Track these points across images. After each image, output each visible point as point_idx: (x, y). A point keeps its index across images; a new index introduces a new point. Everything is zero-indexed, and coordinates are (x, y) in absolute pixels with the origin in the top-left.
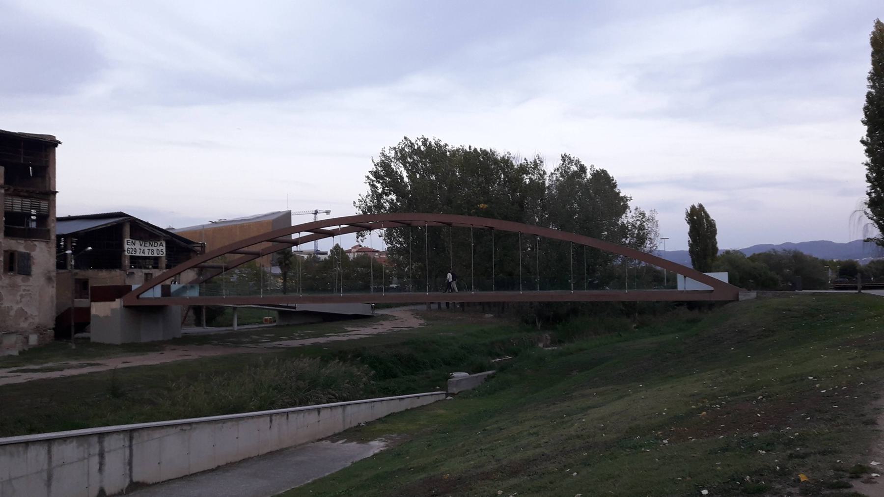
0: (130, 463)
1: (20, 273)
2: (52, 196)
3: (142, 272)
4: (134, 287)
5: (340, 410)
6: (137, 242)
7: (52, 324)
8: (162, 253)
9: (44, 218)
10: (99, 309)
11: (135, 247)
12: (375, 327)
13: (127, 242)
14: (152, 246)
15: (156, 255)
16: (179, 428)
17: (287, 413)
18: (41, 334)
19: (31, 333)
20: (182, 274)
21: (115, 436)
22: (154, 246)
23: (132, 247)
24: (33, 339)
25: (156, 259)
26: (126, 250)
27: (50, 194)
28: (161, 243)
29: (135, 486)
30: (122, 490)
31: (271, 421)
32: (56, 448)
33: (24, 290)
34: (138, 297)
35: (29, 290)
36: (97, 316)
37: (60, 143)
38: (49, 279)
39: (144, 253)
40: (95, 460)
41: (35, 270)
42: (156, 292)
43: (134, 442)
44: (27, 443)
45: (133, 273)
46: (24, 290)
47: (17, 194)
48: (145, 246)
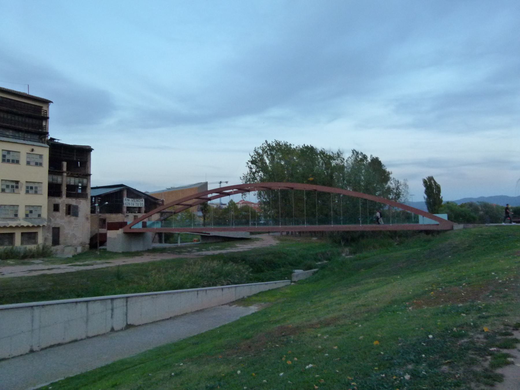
0: (126, 315)
1: (73, 216)
2: (89, 177)
4: (128, 223)
5: (233, 289)
6: (131, 199)
7: (88, 241)
9: (84, 188)
10: (111, 234)
11: (130, 202)
12: (251, 244)
14: (138, 201)
15: (139, 206)
16: (151, 296)
17: (206, 290)
18: (83, 247)
19: (78, 246)
20: (152, 216)
21: (119, 300)
23: (128, 202)
24: (79, 250)
25: (140, 208)
26: (125, 203)
27: (88, 175)
29: (129, 326)
30: (123, 328)
31: (198, 294)
32: (91, 305)
33: (75, 224)
34: (130, 228)
35: (77, 224)
36: (110, 238)
37: (93, 149)
38: (87, 219)
40: (110, 311)
41: (81, 214)
42: (139, 226)
43: (128, 303)
44: (76, 302)
45: (128, 216)
46: (75, 224)
47: (72, 176)
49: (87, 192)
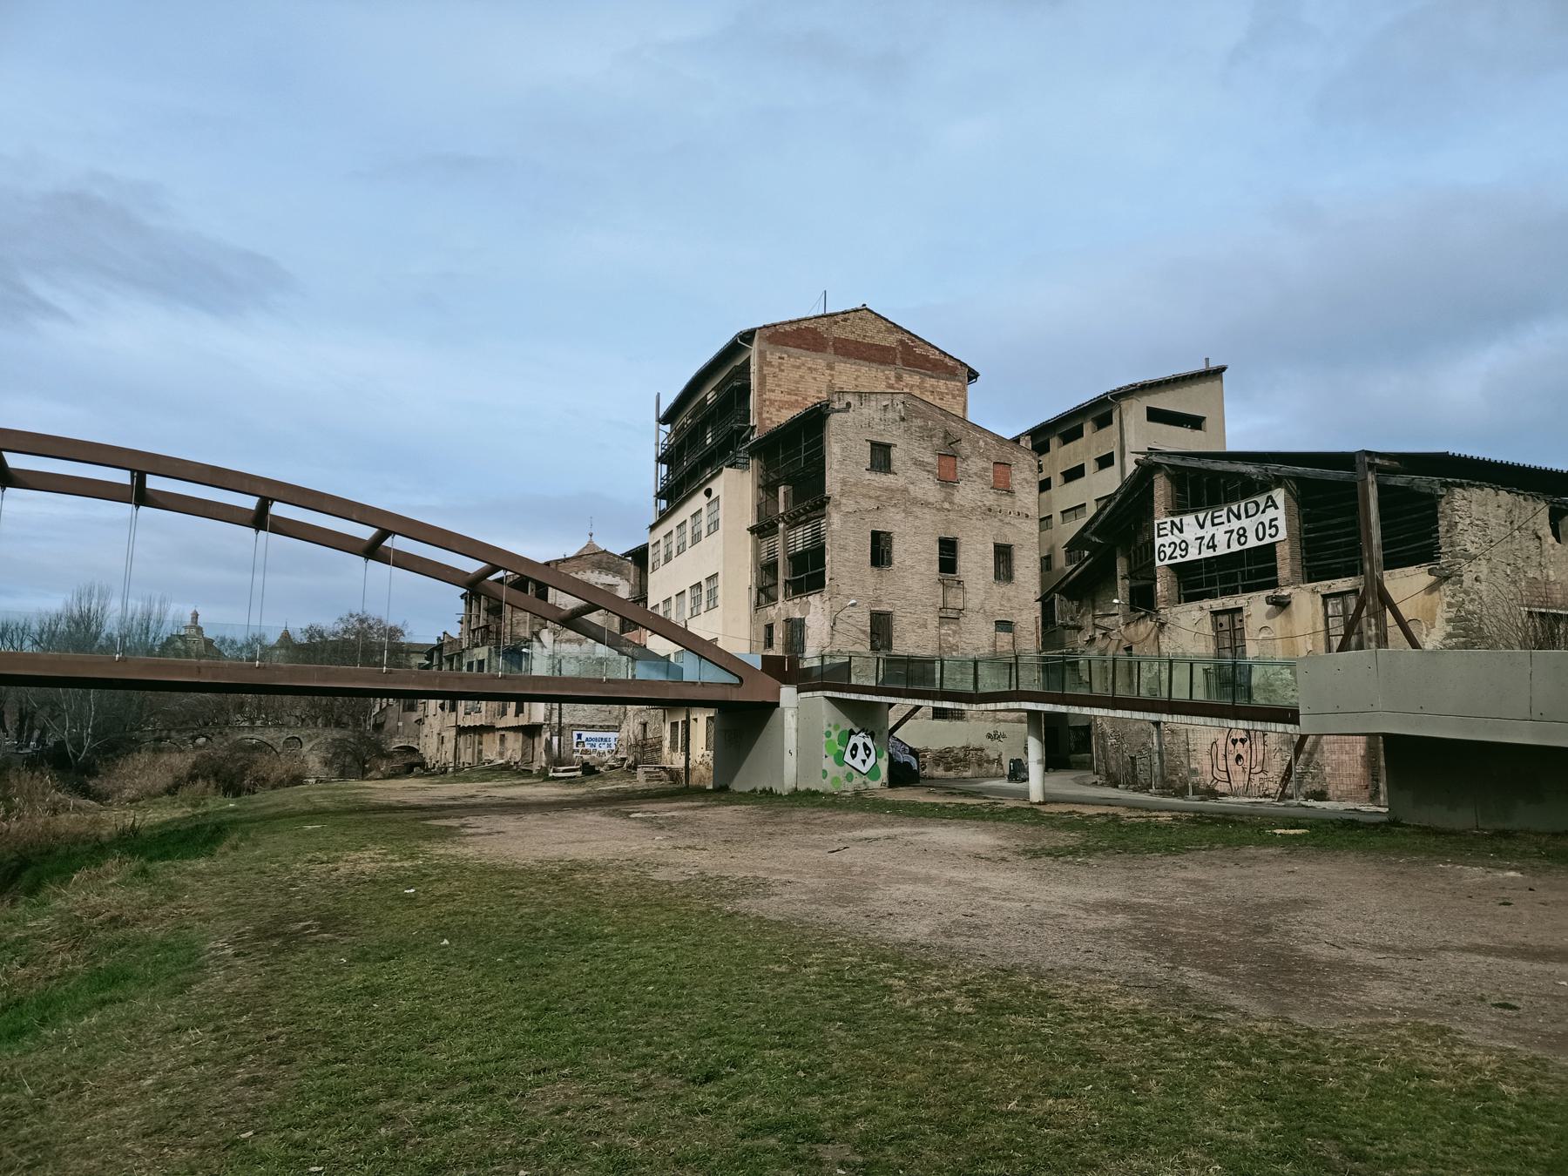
3: (1202, 609)
6: (1189, 520)
8: (1273, 531)
11: (1184, 536)
13: (1159, 530)
14: (1238, 517)
15: (1252, 542)
20: (656, 635)
22: (1247, 517)
28: (1270, 498)
39: (1214, 547)
48: (1213, 525)
49: (241, 638)
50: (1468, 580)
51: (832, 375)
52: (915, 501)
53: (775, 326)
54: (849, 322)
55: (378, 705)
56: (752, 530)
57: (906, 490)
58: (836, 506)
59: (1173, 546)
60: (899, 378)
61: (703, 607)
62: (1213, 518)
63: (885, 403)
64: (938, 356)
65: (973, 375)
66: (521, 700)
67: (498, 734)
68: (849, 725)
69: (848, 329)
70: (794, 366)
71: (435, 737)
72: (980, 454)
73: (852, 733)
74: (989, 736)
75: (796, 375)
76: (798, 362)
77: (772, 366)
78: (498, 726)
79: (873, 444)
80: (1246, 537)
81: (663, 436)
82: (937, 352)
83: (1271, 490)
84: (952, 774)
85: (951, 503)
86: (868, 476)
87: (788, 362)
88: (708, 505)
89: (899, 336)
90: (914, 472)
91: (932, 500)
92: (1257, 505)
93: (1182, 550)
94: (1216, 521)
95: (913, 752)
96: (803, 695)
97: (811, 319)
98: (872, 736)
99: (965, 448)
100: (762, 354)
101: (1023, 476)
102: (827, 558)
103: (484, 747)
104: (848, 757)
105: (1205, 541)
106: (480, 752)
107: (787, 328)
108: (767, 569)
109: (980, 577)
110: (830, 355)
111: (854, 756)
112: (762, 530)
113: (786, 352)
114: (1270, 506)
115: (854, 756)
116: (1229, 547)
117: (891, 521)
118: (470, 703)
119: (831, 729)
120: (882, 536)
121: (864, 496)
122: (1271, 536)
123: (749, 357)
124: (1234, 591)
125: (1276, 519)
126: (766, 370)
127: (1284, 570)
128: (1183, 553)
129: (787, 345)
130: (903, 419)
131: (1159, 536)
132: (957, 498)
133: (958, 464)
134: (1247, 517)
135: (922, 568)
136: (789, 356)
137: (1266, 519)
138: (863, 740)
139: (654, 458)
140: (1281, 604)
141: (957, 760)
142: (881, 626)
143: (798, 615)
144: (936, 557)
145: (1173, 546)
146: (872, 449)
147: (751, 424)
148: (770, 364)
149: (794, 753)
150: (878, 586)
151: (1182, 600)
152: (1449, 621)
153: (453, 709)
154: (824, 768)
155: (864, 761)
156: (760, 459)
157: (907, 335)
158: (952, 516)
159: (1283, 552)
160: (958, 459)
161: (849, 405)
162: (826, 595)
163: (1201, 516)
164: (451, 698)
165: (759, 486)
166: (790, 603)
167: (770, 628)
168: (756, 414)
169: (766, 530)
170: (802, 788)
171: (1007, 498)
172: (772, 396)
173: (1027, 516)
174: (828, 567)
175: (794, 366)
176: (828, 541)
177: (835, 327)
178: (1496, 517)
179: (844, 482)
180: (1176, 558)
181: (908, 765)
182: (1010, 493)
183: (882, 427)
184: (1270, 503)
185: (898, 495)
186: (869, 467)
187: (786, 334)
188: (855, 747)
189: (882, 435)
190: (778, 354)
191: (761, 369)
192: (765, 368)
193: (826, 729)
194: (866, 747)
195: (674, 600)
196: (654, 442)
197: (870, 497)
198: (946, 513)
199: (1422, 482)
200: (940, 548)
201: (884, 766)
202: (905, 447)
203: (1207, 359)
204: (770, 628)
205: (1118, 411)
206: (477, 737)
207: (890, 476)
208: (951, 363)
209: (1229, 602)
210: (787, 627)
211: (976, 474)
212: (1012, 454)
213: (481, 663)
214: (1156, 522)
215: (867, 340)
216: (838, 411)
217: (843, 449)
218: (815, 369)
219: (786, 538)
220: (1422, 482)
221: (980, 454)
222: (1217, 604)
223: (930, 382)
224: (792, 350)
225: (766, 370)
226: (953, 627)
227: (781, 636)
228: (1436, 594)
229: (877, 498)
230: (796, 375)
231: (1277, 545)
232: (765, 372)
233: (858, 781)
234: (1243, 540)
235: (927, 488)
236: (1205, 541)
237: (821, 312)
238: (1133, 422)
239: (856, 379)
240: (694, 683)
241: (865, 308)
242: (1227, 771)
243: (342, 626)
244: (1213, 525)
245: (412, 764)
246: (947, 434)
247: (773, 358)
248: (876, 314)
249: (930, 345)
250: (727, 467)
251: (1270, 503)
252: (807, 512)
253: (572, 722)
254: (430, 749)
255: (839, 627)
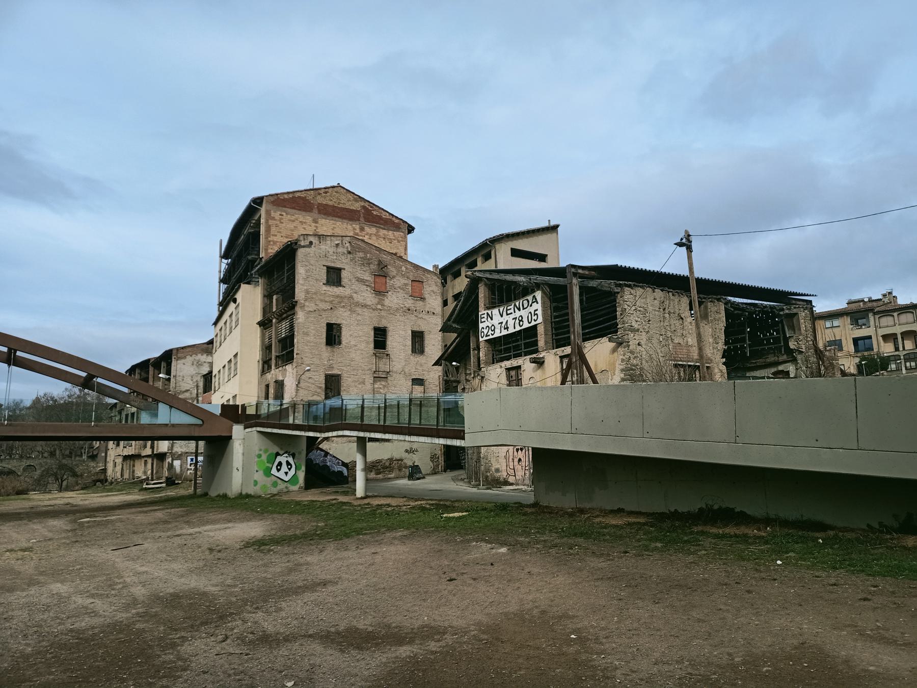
6: (495, 311)
8: (535, 318)
13: (481, 318)
14: (519, 309)
15: (526, 325)
22: (524, 309)
28: (534, 296)
39: (507, 328)
48: (507, 314)
50: (633, 344)
51: (317, 227)
52: (357, 304)
53: (277, 194)
54: (328, 194)
55: (97, 444)
56: (259, 323)
57: (351, 297)
58: (301, 307)
59: (488, 328)
60: (362, 229)
61: (232, 375)
62: (507, 310)
63: (337, 242)
64: (388, 217)
65: (411, 229)
66: (153, 439)
67: (143, 460)
68: (276, 449)
69: (328, 198)
70: (290, 220)
71: (112, 462)
72: (402, 275)
73: (278, 454)
74: (406, 451)
75: (291, 226)
76: (293, 218)
77: (275, 220)
78: (143, 454)
79: (329, 268)
80: (523, 321)
81: (224, 266)
82: (388, 214)
83: (535, 292)
84: (380, 476)
85: (383, 305)
86: (325, 288)
87: (286, 217)
88: (236, 308)
89: (362, 204)
90: (357, 286)
91: (369, 303)
92: (528, 302)
93: (492, 331)
94: (509, 312)
95: (345, 464)
96: (248, 430)
97: (301, 191)
98: (293, 456)
99: (392, 270)
100: (268, 213)
101: (431, 289)
102: (295, 340)
103: (136, 468)
104: (274, 471)
105: (503, 325)
106: (133, 472)
107: (286, 196)
108: (267, 348)
109: (402, 351)
110: (315, 214)
111: (278, 470)
112: (264, 324)
113: (285, 211)
114: (534, 302)
115: (278, 470)
116: (515, 328)
117: (341, 316)
118: (126, 442)
119: (261, 452)
120: (334, 326)
121: (321, 301)
122: (535, 321)
123: (261, 215)
124: (519, 355)
125: (537, 310)
126: (271, 222)
127: (541, 343)
128: (493, 333)
129: (285, 207)
130: (349, 253)
131: (481, 322)
132: (387, 302)
133: (388, 281)
134: (524, 309)
135: (363, 346)
136: (287, 214)
137: (532, 309)
138: (286, 459)
139: (217, 280)
140: (540, 363)
141: (385, 467)
142: (333, 384)
143: (281, 378)
144: (372, 339)
145: (488, 328)
146: (327, 270)
147: (261, 257)
148: (273, 219)
149: (241, 469)
150: (330, 358)
151: (495, 362)
152: (622, 370)
153: (118, 445)
154: (255, 479)
155: (286, 473)
156: (265, 278)
157: (368, 203)
158: (383, 313)
159: (541, 330)
160: (388, 278)
161: (311, 243)
162: (294, 364)
163: (501, 309)
164: (117, 439)
165: (265, 296)
166: (277, 370)
167: (267, 386)
168: (263, 250)
169: (267, 324)
170: (244, 493)
171: (420, 302)
172: (275, 239)
173: (434, 313)
174: (296, 346)
175: (290, 220)
176: (296, 329)
177: (319, 197)
178: (652, 305)
179: (307, 292)
180: (489, 335)
181: (341, 473)
182: (423, 299)
183: (335, 257)
184: (534, 300)
185: (346, 300)
186: (325, 282)
187: (284, 200)
188: (280, 464)
189: (334, 262)
190: (279, 213)
191: (267, 221)
192: (270, 221)
193: (257, 452)
194: (288, 463)
195: (221, 370)
196: (218, 270)
197: (326, 302)
198: (379, 311)
199: (607, 284)
200: (375, 334)
201: (301, 475)
202: (351, 270)
203: (549, 221)
204: (267, 386)
205: (494, 250)
206: (132, 462)
207: (341, 288)
208: (397, 221)
209: (514, 363)
210: (276, 386)
211: (399, 287)
212: (424, 275)
213: (133, 414)
214: (480, 313)
215: (341, 206)
216: (304, 247)
217: (307, 271)
218: (305, 223)
219: (276, 328)
220: (607, 284)
221: (402, 275)
222: (508, 364)
223: (383, 232)
224: (289, 210)
225: (271, 222)
226: (383, 383)
227: (272, 392)
228: (616, 354)
229: (331, 302)
230: (291, 226)
231: (538, 326)
232: (270, 223)
233: (282, 486)
234: (521, 323)
235: (367, 296)
236: (503, 325)
237: (312, 187)
238: (502, 257)
239: (333, 229)
240: (167, 425)
241: (339, 186)
242: (514, 469)
243: (67, 393)
244: (507, 314)
245: (101, 481)
246: (380, 263)
247: (276, 214)
248: (346, 190)
249: (383, 209)
250: (244, 284)
251: (534, 300)
252: (286, 312)
253: (187, 451)
254: (114, 470)
255: (302, 384)
